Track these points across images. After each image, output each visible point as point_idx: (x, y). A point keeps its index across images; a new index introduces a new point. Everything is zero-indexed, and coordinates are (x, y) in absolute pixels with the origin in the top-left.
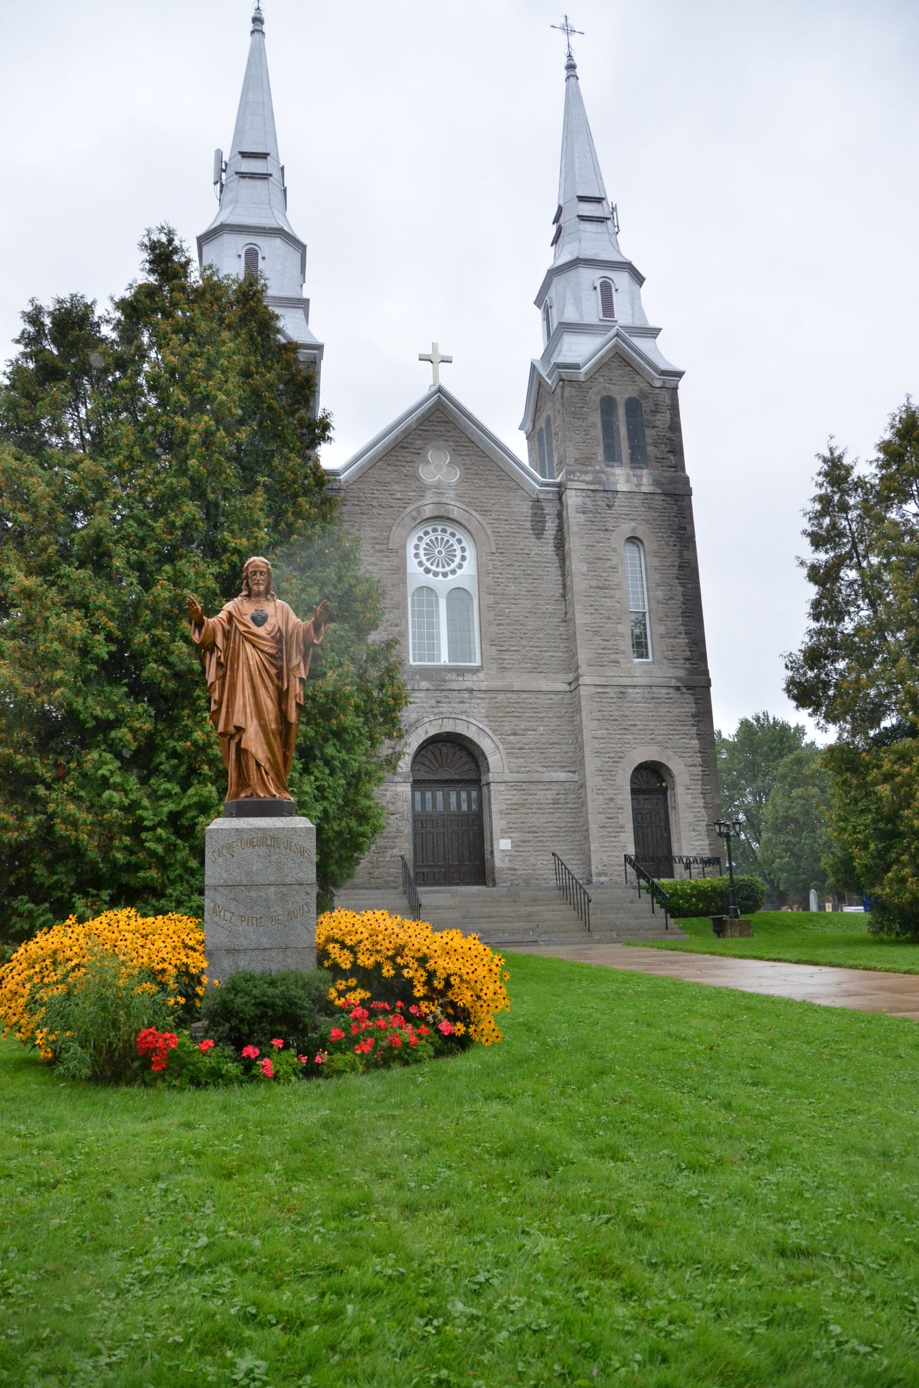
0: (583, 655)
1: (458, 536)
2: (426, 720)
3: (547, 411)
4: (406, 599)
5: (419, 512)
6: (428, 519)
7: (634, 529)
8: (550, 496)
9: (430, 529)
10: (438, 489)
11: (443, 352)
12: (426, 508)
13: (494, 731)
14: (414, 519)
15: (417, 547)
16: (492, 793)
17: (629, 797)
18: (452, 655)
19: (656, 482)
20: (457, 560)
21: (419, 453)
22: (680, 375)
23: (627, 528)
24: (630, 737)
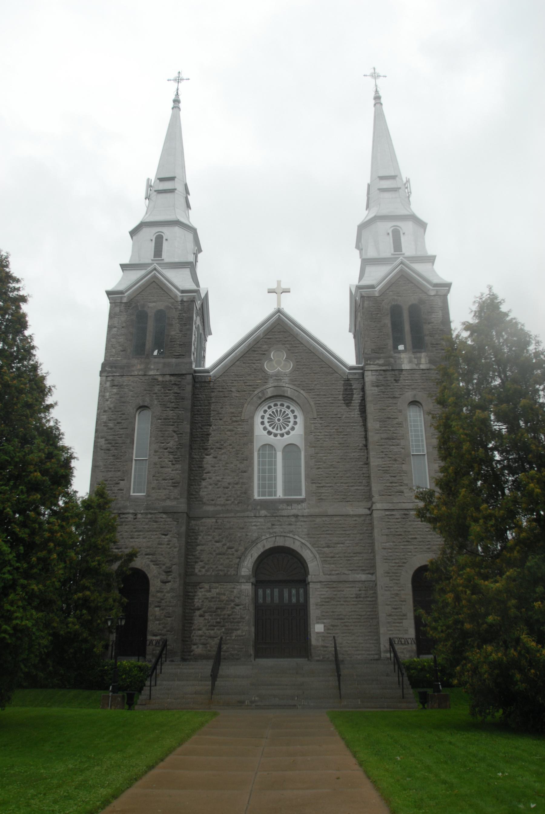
0: (376, 487)
1: (292, 408)
2: (263, 537)
3: (359, 319)
4: (252, 453)
5: (263, 394)
6: (270, 398)
7: (415, 396)
8: (357, 376)
9: (272, 405)
10: (278, 377)
11: (284, 286)
12: (268, 390)
13: (313, 545)
14: (260, 398)
15: (263, 417)
16: (311, 590)
17: (411, 593)
18: (286, 491)
19: (431, 362)
20: (291, 425)
21: (265, 354)
22: (448, 286)
23: (409, 395)
24: (412, 547)
